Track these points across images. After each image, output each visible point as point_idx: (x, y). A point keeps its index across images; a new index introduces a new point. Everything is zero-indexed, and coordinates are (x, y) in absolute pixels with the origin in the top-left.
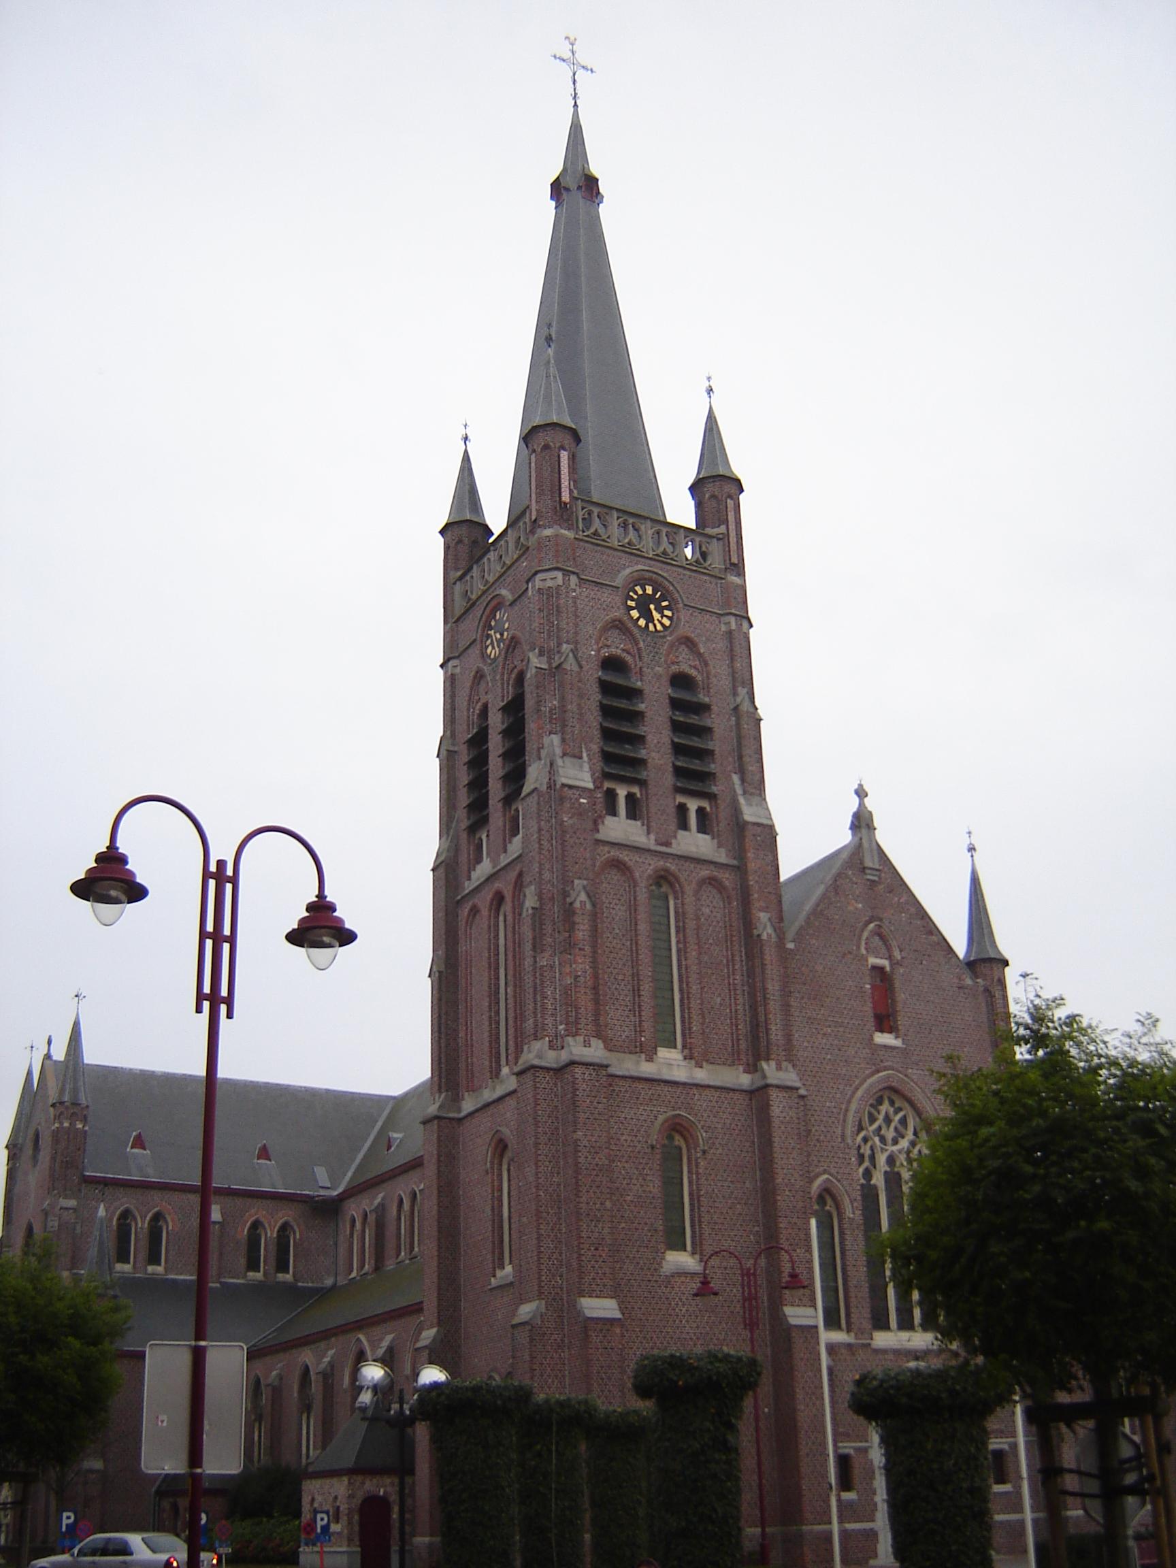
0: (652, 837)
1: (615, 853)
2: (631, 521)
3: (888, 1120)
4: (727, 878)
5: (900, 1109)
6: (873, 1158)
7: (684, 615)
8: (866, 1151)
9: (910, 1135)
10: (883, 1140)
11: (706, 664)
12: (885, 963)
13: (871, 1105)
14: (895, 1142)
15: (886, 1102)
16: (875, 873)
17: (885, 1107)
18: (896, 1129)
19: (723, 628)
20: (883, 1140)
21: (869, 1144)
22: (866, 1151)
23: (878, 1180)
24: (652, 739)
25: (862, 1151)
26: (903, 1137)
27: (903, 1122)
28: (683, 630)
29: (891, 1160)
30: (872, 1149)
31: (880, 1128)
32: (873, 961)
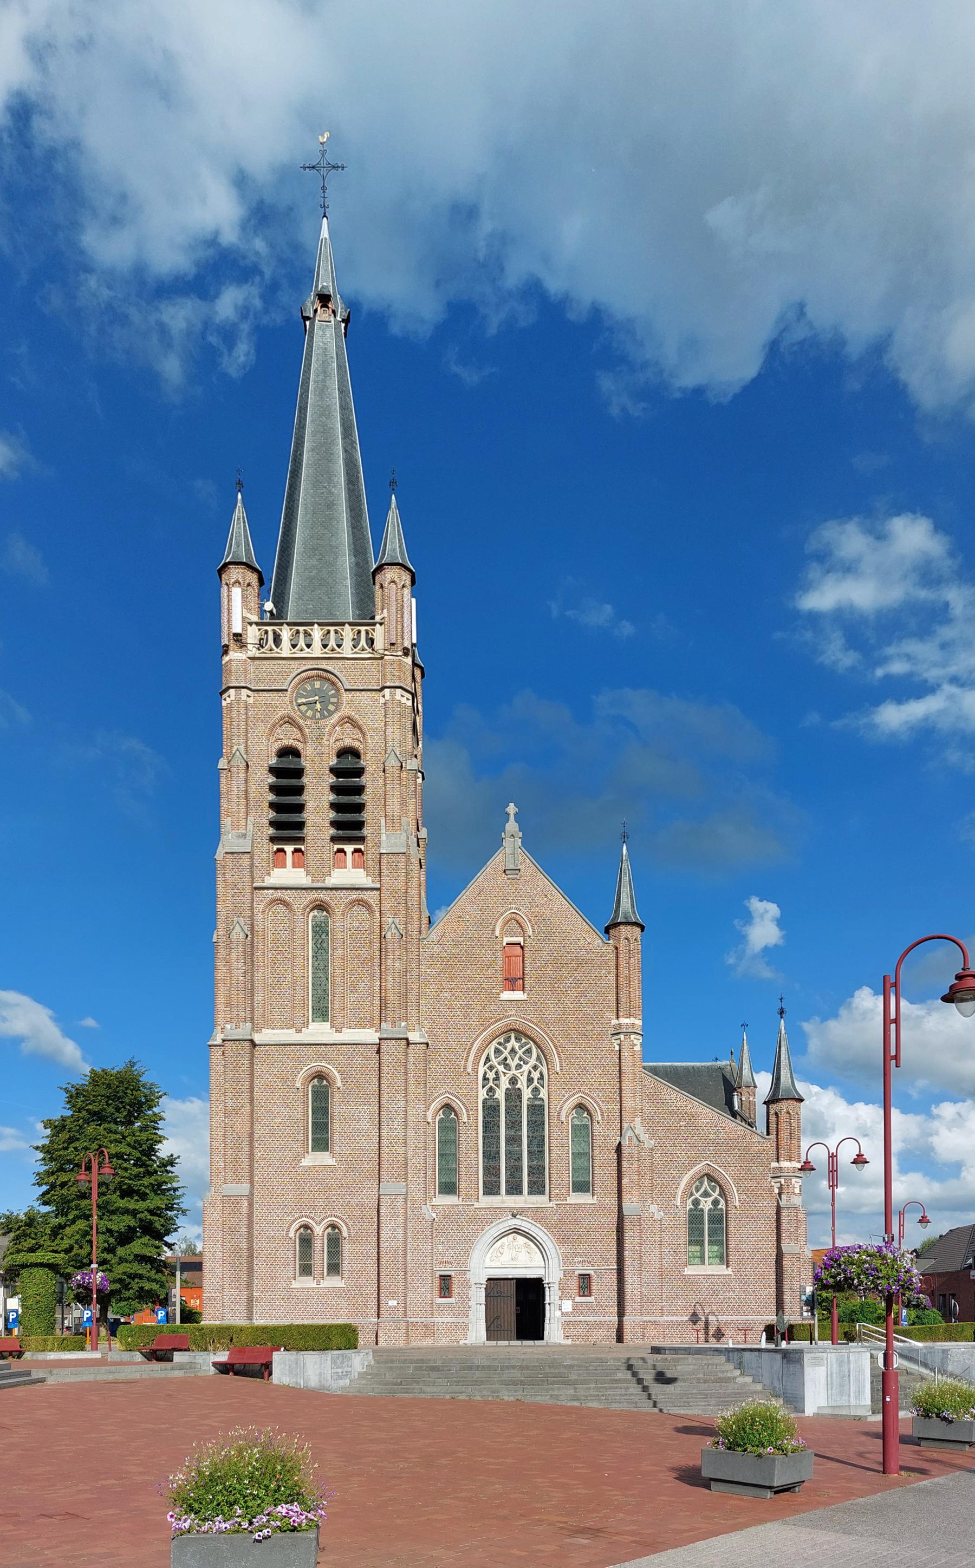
0: (309, 878)
1: (279, 894)
2: (301, 629)
3: (513, 1051)
4: (371, 897)
5: (526, 1044)
6: (497, 1078)
7: (346, 697)
8: (491, 1075)
9: (533, 1061)
10: (507, 1067)
11: (364, 734)
12: (521, 940)
13: (500, 1044)
14: (519, 1067)
15: (513, 1039)
16: (514, 872)
17: (513, 1043)
18: (521, 1059)
19: (382, 700)
20: (507, 1067)
21: (494, 1071)
22: (491, 1075)
23: (500, 1095)
24: (310, 805)
25: (487, 1076)
26: (526, 1063)
27: (529, 1051)
28: (345, 711)
29: (513, 1081)
30: (497, 1073)
31: (506, 1059)
32: (507, 940)
